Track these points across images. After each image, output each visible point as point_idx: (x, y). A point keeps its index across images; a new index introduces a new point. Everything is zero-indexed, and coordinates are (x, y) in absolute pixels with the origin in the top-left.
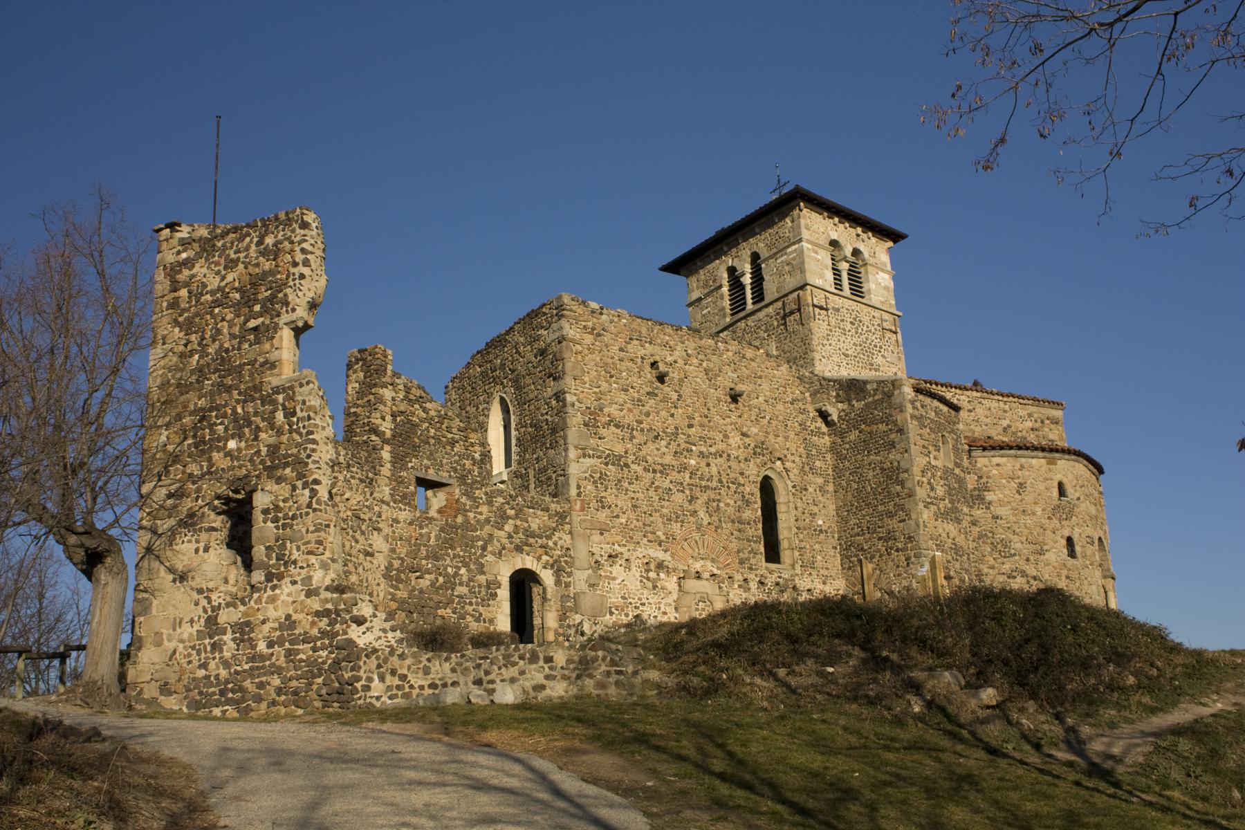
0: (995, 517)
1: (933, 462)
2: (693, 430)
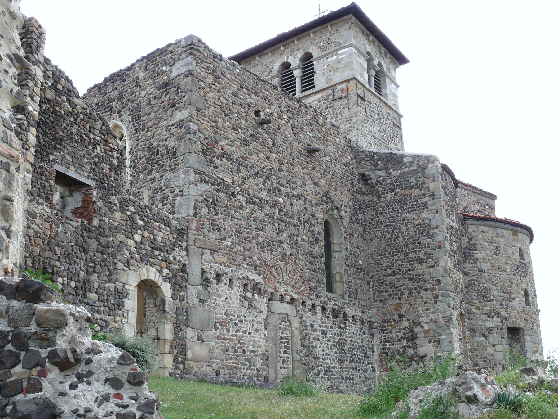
0: (481, 271)
2: (282, 173)
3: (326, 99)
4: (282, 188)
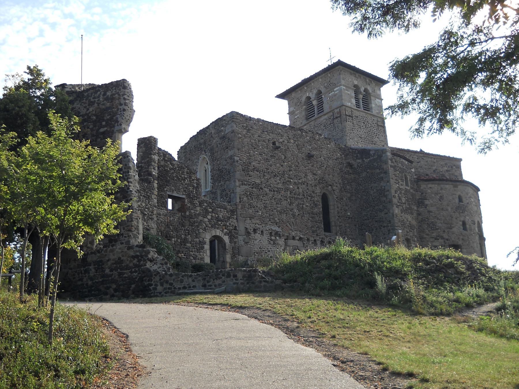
0: (429, 212)
2: (291, 172)
3: (330, 118)
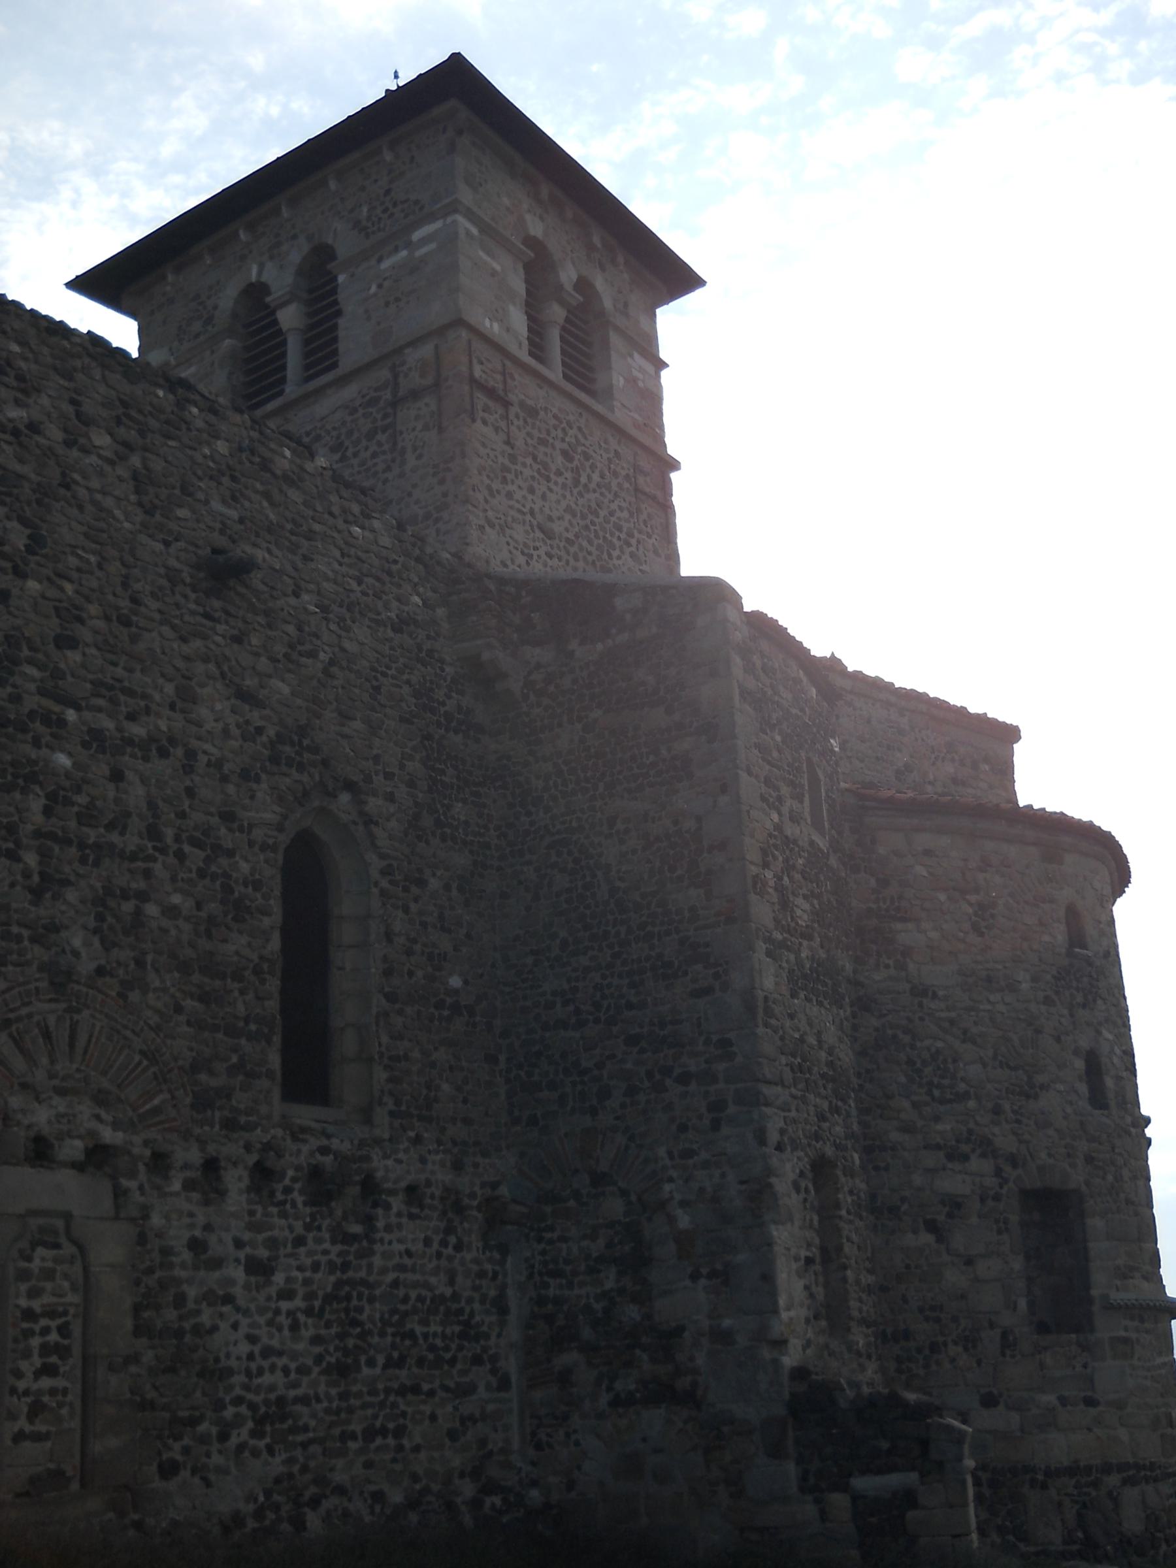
1: (790, 830)
2: (74, 656)
3: (373, 402)
4: (71, 715)
